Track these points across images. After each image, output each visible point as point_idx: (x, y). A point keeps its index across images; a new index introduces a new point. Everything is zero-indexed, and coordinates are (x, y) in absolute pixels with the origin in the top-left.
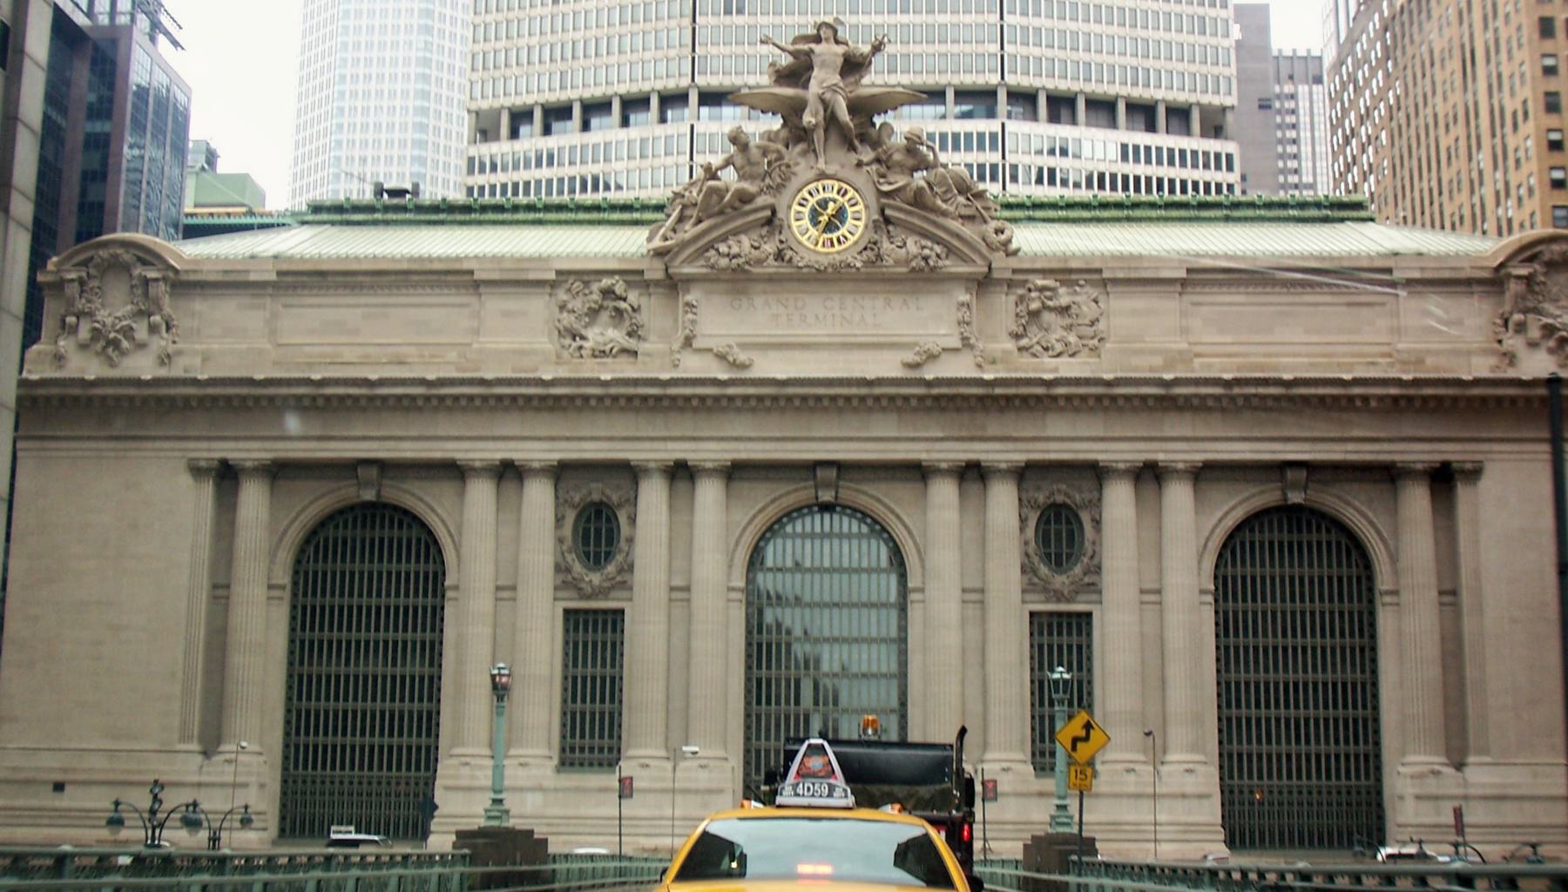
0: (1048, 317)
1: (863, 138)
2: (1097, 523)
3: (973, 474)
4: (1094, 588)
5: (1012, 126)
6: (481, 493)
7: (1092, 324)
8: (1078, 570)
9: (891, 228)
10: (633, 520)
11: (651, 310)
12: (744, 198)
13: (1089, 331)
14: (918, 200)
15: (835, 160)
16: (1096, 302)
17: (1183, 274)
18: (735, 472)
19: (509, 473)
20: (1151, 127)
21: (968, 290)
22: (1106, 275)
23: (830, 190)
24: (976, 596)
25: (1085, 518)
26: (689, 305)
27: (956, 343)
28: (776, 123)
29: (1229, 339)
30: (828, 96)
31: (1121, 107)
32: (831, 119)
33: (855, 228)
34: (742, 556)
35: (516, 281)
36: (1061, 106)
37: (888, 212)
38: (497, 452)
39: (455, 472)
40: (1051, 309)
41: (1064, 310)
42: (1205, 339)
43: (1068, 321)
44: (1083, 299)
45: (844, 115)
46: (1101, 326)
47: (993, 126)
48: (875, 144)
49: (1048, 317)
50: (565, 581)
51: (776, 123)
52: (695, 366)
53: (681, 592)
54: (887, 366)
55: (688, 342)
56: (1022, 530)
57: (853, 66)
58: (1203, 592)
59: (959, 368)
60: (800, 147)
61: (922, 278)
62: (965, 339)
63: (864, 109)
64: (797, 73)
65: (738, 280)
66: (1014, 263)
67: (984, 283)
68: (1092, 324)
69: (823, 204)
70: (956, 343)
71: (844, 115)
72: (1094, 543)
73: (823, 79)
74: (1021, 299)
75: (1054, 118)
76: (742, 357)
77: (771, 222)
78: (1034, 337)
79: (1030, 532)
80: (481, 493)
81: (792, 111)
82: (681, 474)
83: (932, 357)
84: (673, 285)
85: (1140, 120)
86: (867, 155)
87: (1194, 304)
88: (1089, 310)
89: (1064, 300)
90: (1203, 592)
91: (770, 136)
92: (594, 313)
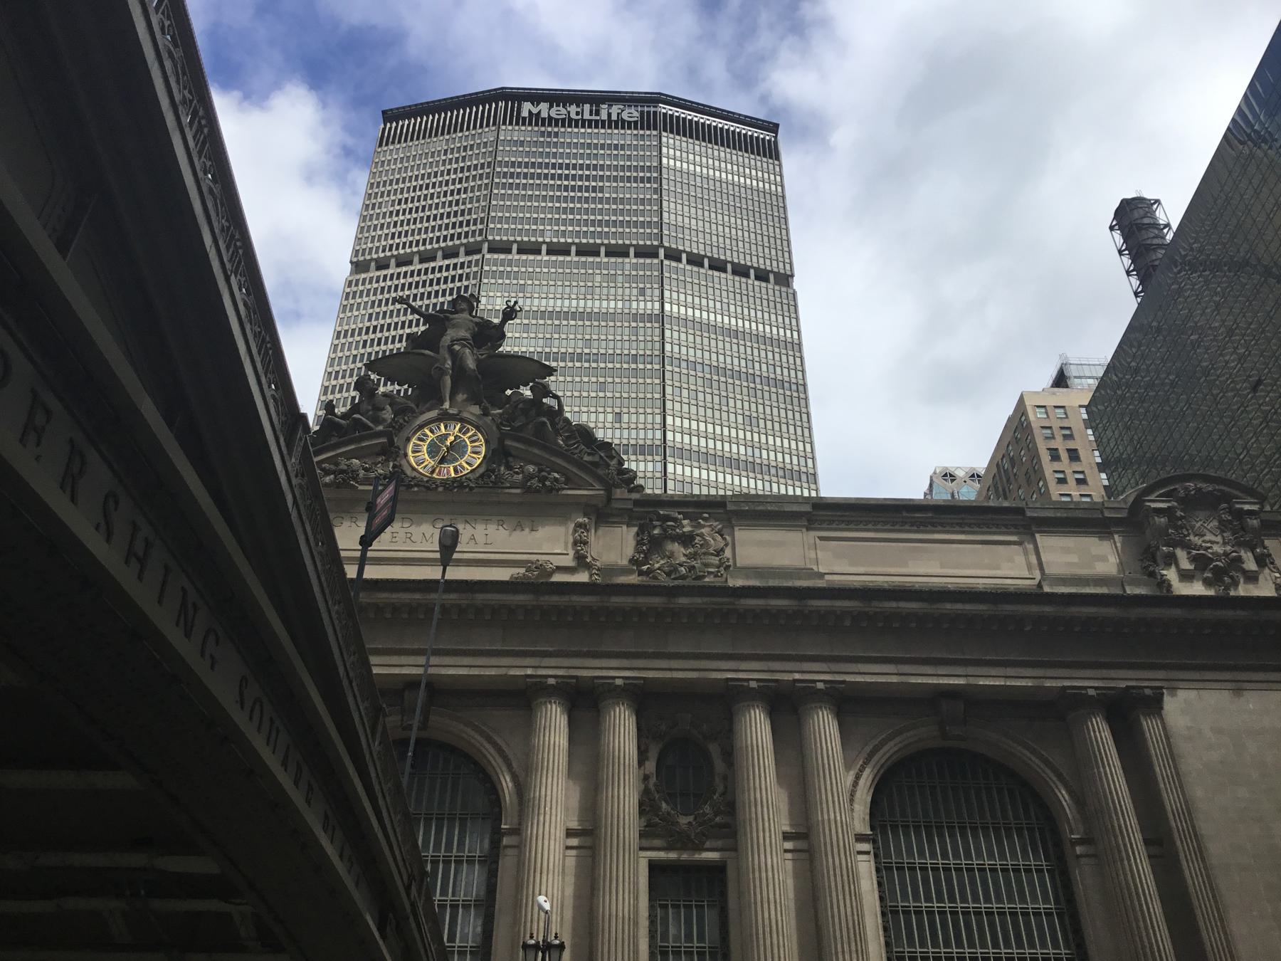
7: (719, 552)
8: (707, 809)
9: (510, 459)
13: (715, 560)
16: (720, 533)
17: (808, 508)
21: (585, 515)
22: (730, 507)
25: (714, 749)
29: (862, 570)
30: (457, 347)
37: (508, 442)
40: (675, 538)
42: (837, 569)
43: (691, 550)
46: (728, 553)
56: (641, 763)
58: (860, 838)
62: (580, 558)
67: (603, 514)
68: (719, 552)
70: (568, 561)
72: (725, 778)
79: (651, 766)
87: (821, 538)
88: (715, 542)
90: (860, 838)
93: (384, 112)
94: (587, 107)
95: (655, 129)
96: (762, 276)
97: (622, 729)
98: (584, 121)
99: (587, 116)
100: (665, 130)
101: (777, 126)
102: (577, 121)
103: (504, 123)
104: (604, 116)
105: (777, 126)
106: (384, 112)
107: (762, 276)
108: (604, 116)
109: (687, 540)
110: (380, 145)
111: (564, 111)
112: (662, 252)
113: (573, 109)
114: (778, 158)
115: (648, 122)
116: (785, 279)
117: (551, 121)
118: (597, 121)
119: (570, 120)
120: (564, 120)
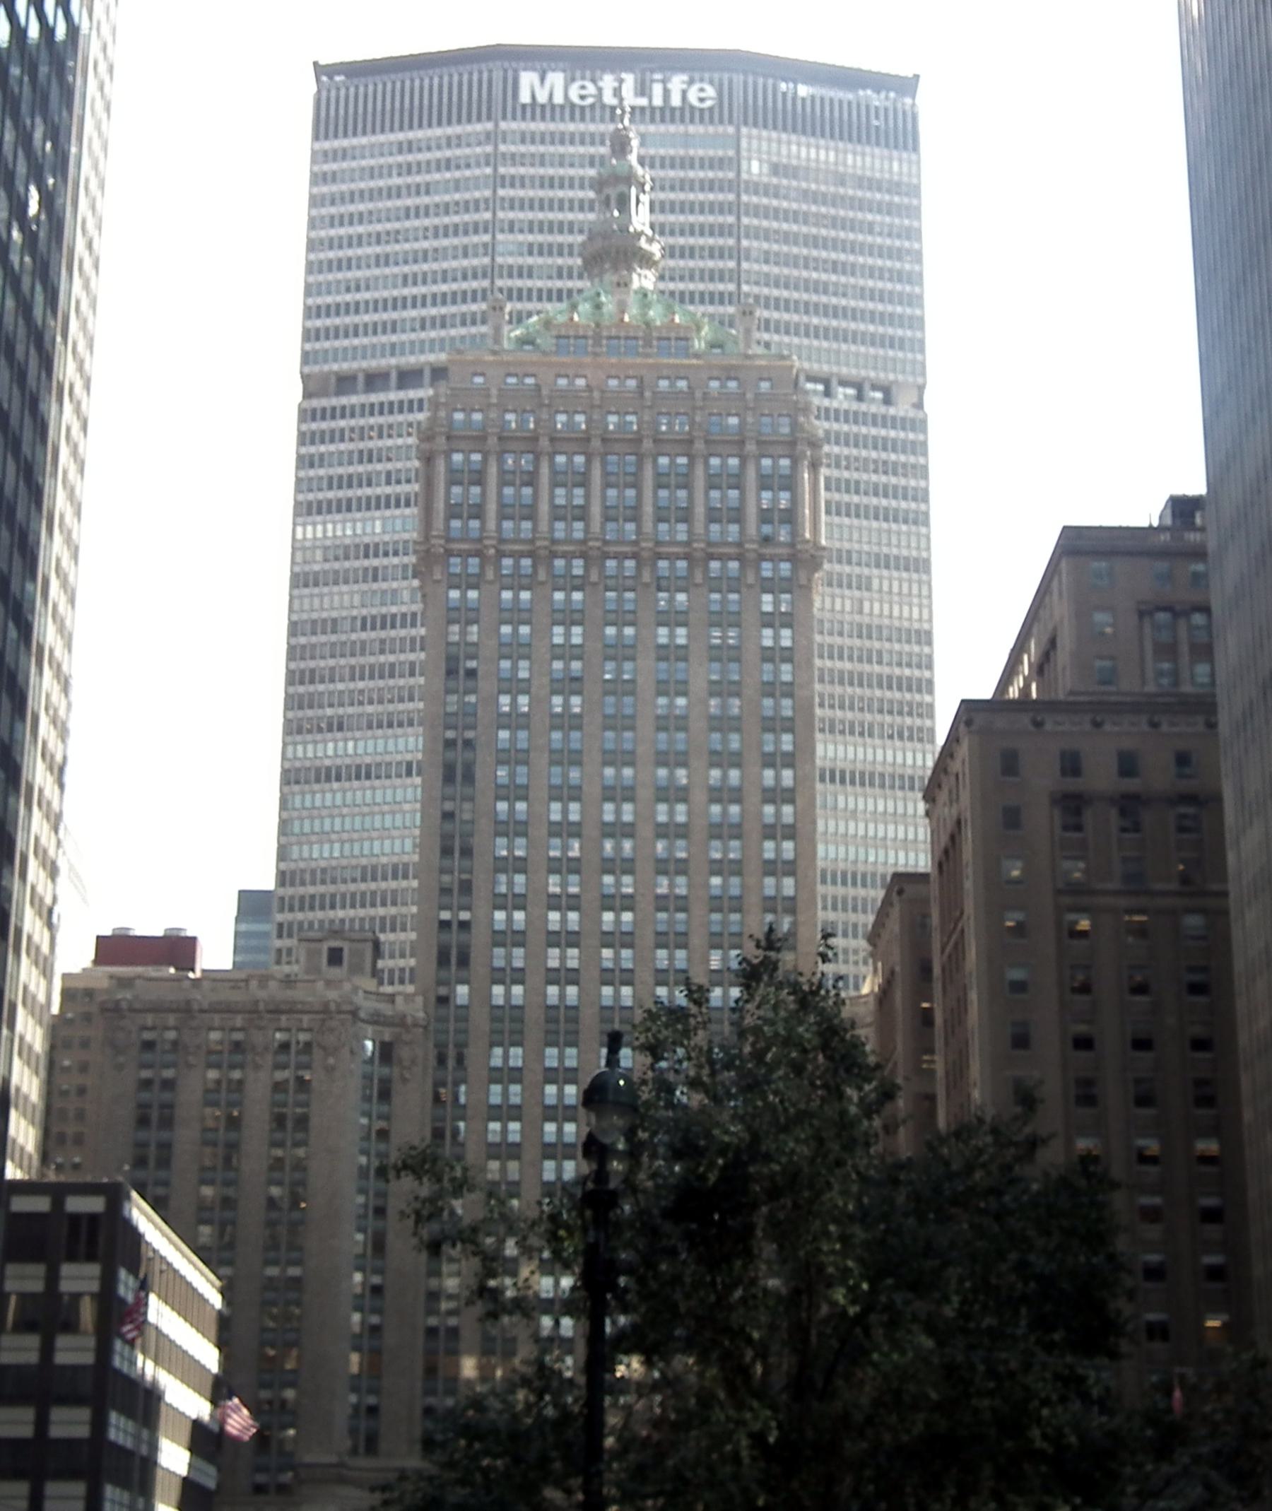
93: (315, 64)
94: (629, 79)
95: (731, 122)
100: (746, 123)
101: (917, 77)
102: (613, 109)
103: (504, 118)
104: (658, 101)
105: (917, 77)
106: (315, 64)
108: (658, 101)
110: (316, 137)
111: (591, 89)
113: (608, 82)
117: (572, 111)
118: (642, 109)
119: (603, 106)
120: (592, 106)
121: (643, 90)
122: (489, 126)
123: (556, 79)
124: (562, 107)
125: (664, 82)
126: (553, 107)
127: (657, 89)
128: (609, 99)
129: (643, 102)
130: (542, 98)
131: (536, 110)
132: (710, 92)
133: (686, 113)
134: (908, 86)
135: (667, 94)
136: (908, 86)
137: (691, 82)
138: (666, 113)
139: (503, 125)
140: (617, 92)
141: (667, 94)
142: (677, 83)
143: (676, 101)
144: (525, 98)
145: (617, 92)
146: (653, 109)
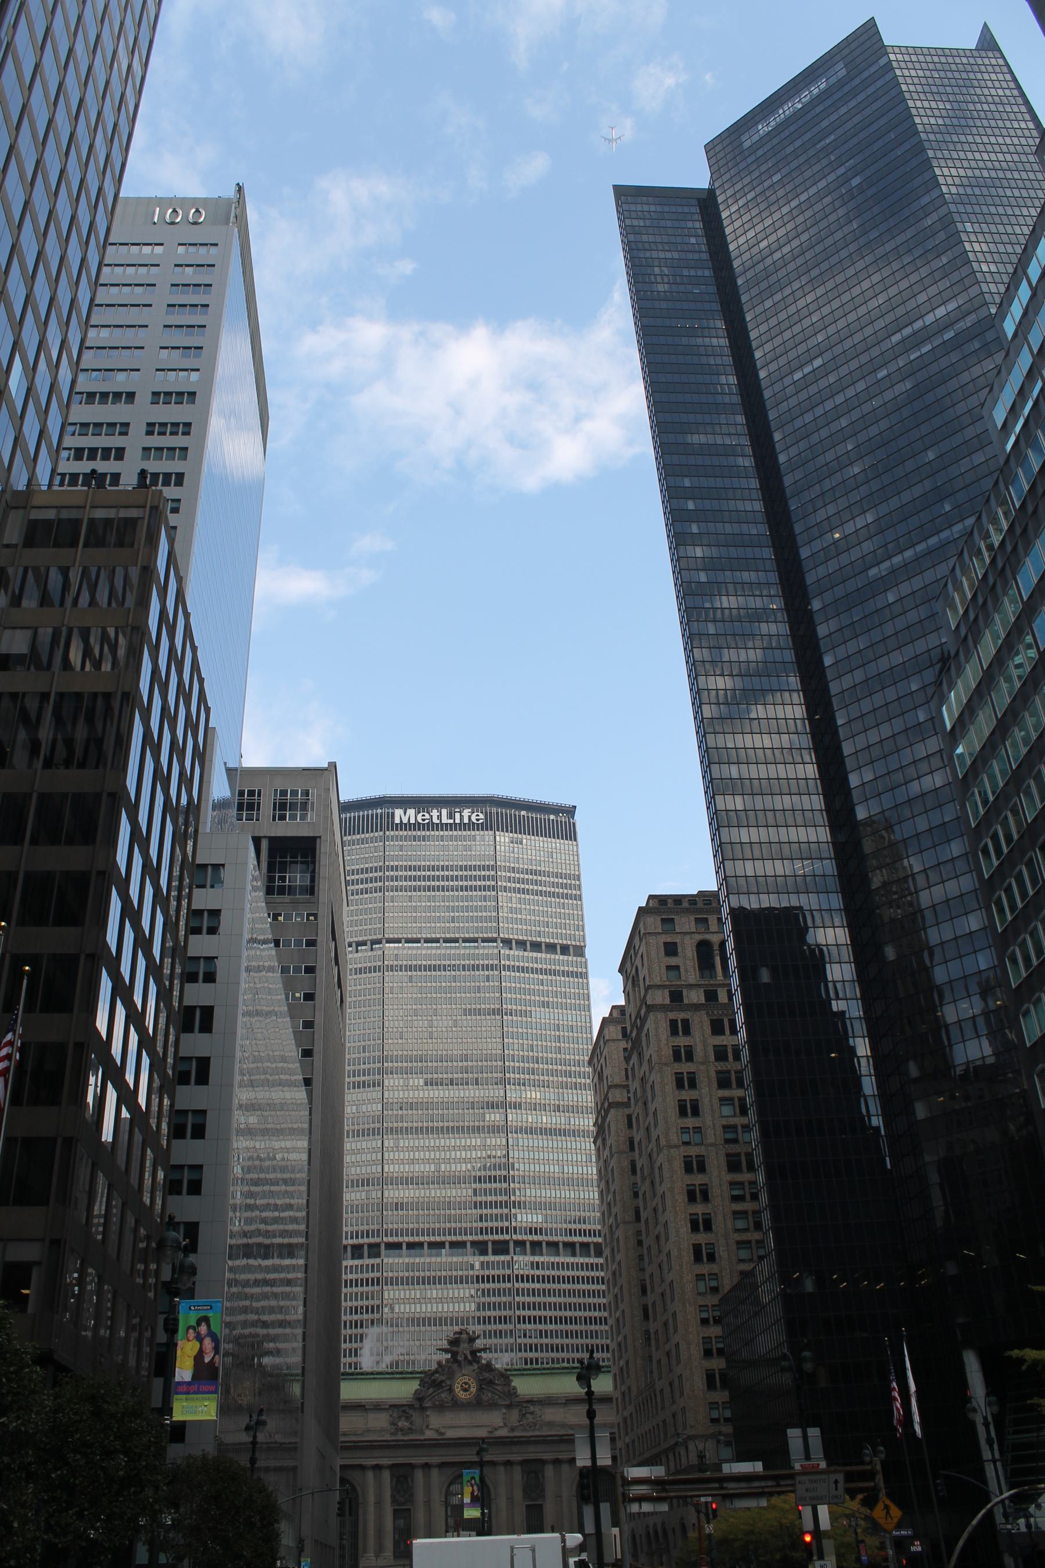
0: (528, 1415)
1: (475, 1361)
2: (543, 1477)
3: (508, 1463)
4: (544, 1497)
5: (515, 1258)
6: (370, 1475)
10: (412, 1481)
11: (416, 1417)
12: (442, 1381)
14: (491, 1382)
15: (468, 1369)
18: (442, 1465)
19: (378, 1467)
20: (574, 1255)
23: (466, 1379)
24: (510, 1499)
26: (428, 1416)
27: (502, 1424)
28: (449, 1356)
31: (561, 1245)
32: (466, 1358)
33: (473, 1390)
34: (444, 1490)
35: (377, 1407)
36: (536, 1246)
38: (374, 1462)
39: (362, 1468)
41: (532, 1413)
44: (536, 1409)
45: (469, 1357)
47: (508, 1258)
48: (478, 1362)
49: (528, 1415)
50: (394, 1500)
51: (449, 1356)
52: (429, 1434)
53: (428, 1503)
54: (482, 1433)
55: (427, 1427)
57: (472, 1340)
59: (503, 1432)
60: (456, 1365)
61: (493, 1406)
62: (505, 1425)
63: (473, 1353)
64: (454, 1342)
65: (441, 1407)
66: (517, 1399)
67: (509, 1407)
69: (466, 1383)
70: (502, 1424)
71: (469, 1357)
73: (464, 1347)
74: (520, 1410)
75: (533, 1253)
76: (443, 1431)
77: (451, 1390)
78: (525, 1422)
80: (370, 1475)
81: (454, 1354)
82: (427, 1466)
83: (496, 1429)
84: (423, 1409)
85: (569, 1250)
86: (476, 1366)
88: (539, 1413)
89: (532, 1408)
91: (447, 1360)
92: (400, 1417)
94: (444, 812)
96: (565, 950)
97: (517, 1473)
98: (442, 824)
99: (445, 820)
101: (575, 807)
105: (575, 807)
107: (565, 950)
108: (458, 821)
109: (532, 1413)
111: (427, 816)
112: (499, 941)
113: (435, 813)
114: (575, 840)
115: (485, 826)
116: (580, 951)
117: (417, 826)
119: (433, 824)
121: (451, 816)
122: (381, 833)
123: (411, 812)
124: (414, 824)
125: (460, 812)
126: (410, 824)
127: (457, 815)
128: (436, 820)
129: (451, 821)
130: (405, 821)
131: (402, 826)
132: (482, 816)
133: (471, 826)
134: (571, 811)
135: (461, 817)
136: (571, 811)
137: (473, 812)
138: (462, 826)
139: (387, 833)
140: (440, 817)
141: (461, 817)
142: (466, 813)
143: (466, 821)
144: (397, 821)
145: (440, 817)
146: (456, 824)
